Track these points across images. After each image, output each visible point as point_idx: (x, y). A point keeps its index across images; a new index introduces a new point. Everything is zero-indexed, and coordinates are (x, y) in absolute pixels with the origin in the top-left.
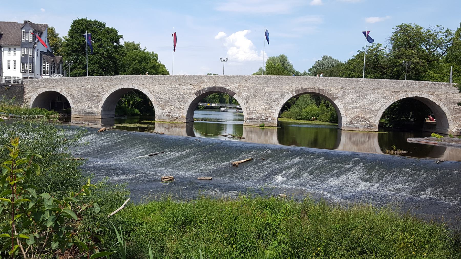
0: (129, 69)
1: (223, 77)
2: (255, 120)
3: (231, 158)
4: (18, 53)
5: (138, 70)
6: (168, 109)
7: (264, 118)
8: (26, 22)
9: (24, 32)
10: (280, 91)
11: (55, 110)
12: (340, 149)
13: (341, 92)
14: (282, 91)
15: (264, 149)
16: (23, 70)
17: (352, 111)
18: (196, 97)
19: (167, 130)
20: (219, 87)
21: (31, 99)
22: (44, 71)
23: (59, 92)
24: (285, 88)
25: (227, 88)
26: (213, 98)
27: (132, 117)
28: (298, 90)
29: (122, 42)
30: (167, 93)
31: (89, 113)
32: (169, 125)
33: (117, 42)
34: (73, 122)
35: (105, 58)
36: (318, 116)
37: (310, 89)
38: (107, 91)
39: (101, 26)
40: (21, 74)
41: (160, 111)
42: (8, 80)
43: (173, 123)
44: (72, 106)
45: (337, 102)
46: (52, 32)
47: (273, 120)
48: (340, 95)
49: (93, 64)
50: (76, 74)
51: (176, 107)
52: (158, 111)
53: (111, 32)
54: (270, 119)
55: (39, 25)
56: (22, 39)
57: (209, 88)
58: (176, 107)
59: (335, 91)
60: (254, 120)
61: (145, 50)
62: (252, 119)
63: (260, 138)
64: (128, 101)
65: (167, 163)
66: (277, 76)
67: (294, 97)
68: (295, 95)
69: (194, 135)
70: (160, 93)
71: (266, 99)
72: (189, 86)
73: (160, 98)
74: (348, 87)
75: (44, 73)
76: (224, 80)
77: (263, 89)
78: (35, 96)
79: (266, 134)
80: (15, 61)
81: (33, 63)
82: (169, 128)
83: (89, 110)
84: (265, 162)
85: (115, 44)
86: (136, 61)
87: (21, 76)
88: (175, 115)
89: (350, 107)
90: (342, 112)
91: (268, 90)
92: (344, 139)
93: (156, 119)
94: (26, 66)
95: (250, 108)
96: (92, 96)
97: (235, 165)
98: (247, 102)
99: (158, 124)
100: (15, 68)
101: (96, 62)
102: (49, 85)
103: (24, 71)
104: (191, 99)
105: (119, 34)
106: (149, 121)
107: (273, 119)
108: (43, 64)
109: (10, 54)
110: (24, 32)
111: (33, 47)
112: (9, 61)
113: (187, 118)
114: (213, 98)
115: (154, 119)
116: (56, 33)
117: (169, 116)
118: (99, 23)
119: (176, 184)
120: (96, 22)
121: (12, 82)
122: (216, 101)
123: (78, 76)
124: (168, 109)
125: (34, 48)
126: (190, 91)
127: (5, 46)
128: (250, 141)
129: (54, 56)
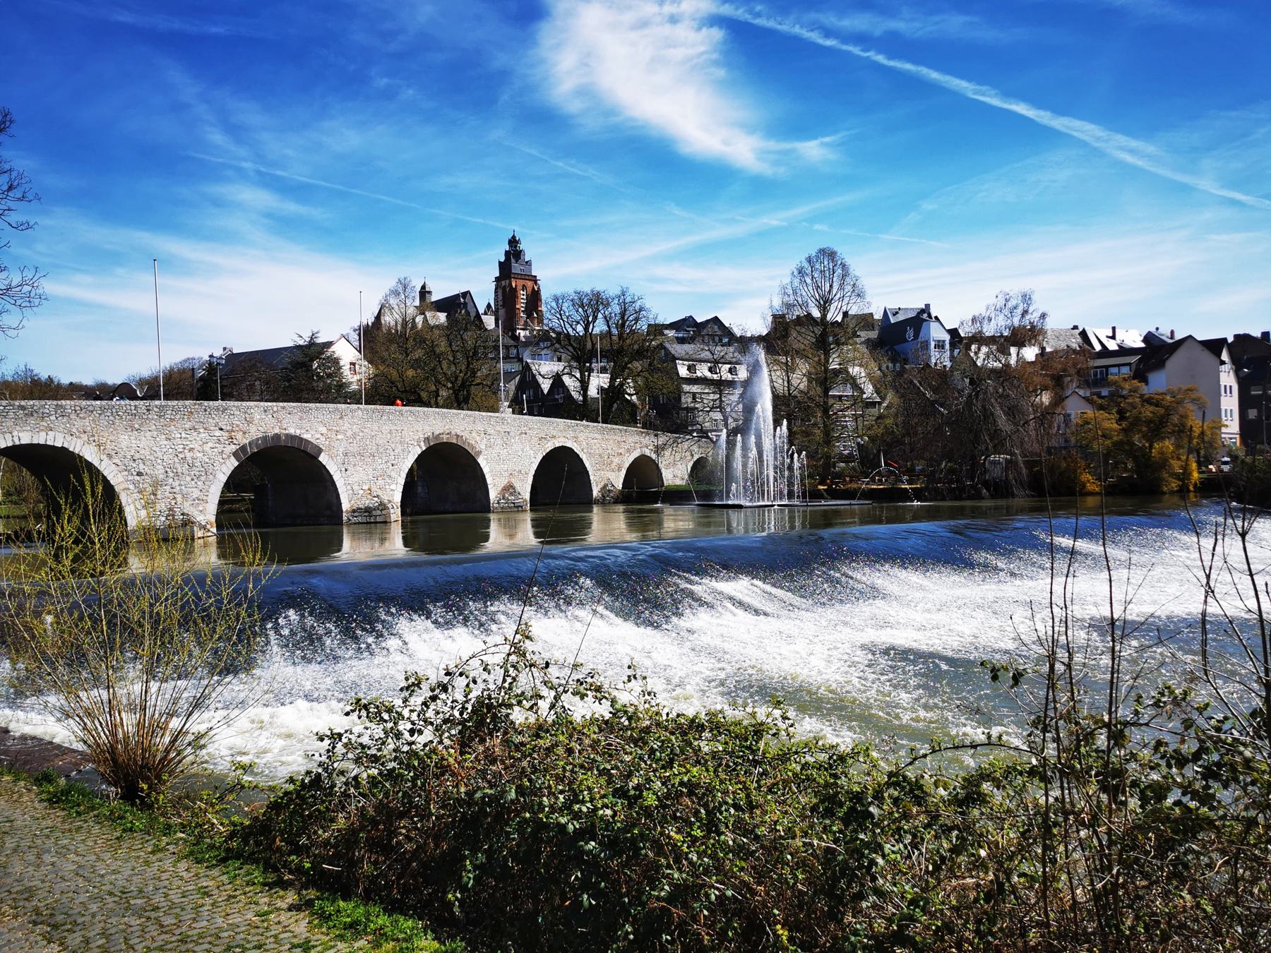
25: (305, 436)
30: (160, 454)
57: (265, 438)
70: (137, 456)
72: (218, 433)
73: (139, 474)
126: (220, 448)
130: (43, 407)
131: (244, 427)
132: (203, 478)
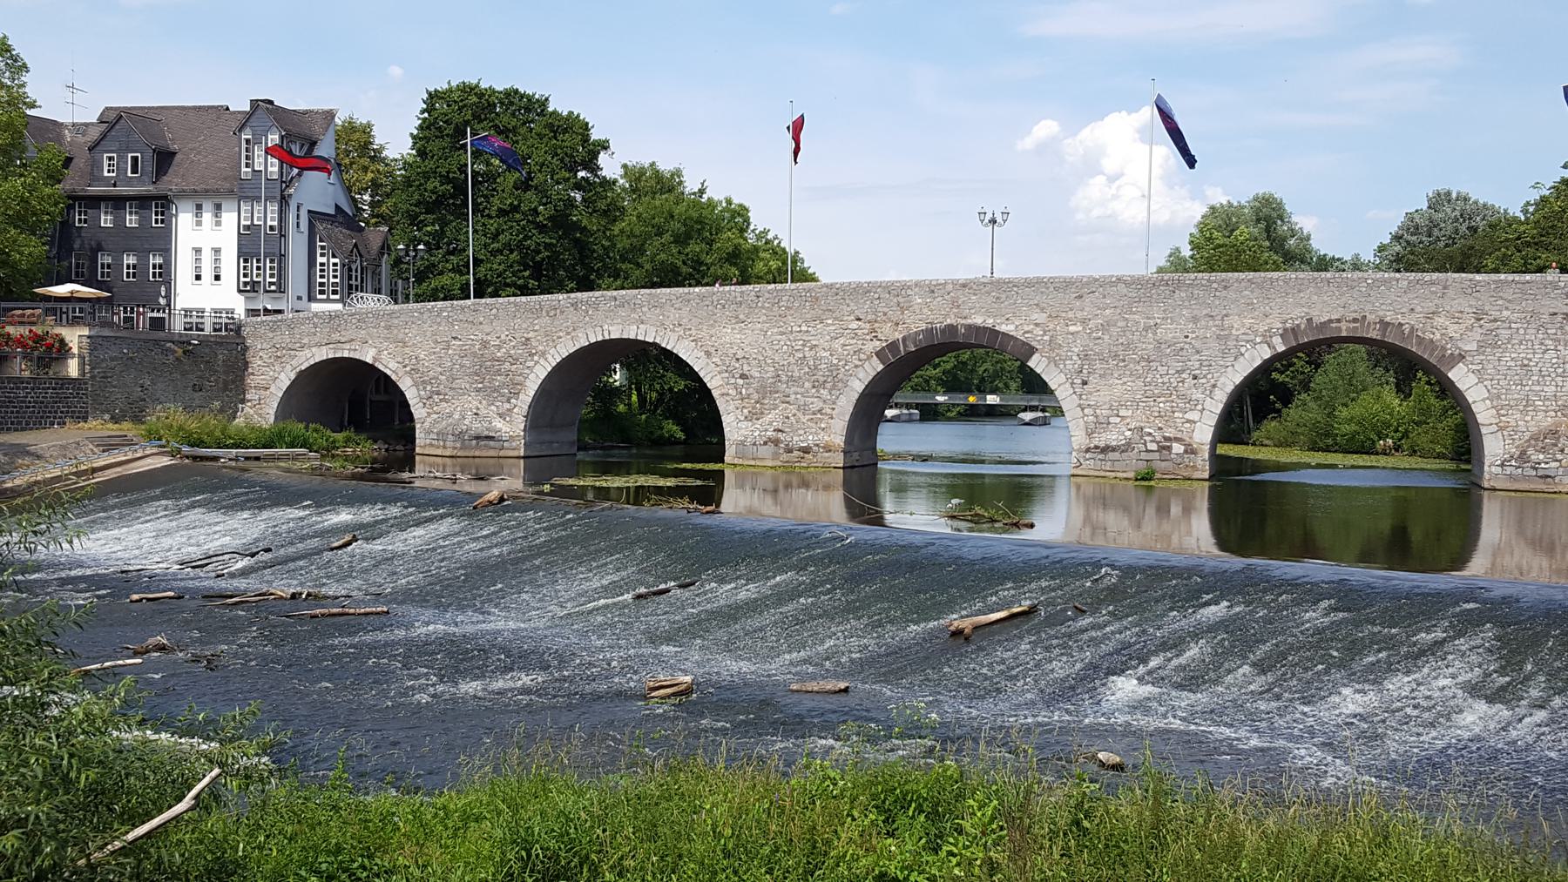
0: (639, 265)
1: (985, 285)
2: (1116, 455)
3: (950, 606)
4: (229, 218)
5: (675, 271)
6: (772, 418)
7: (1153, 447)
8: (255, 104)
9: (248, 141)
10: (1218, 337)
11: (358, 430)
12: (1478, 566)
13: (1477, 334)
14: (1227, 337)
15: (1097, 565)
16: (246, 284)
17: (1524, 412)
18: (881, 367)
19: (769, 500)
20: (969, 327)
21: (273, 389)
22: (322, 284)
23: (369, 360)
24: (1238, 324)
25: (1004, 328)
26: (997, 375)
27: (654, 451)
28: (1294, 331)
29: (609, 166)
31: (478, 438)
32: (775, 480)
33: (591, 164)
34: (424, 475)
35: (541, 228)
36: (1406, 435)
37: (1343, 326)
38: (543, 354)
39: (534, 106)
40: (241, 298)
41: (743, 425)
42: (194, 320)
43: (793, 472)
44: (418, 411)
45: (1460, 376)
46: (358, 140)
47: (1194, 452)
48: (1474, 346)
49: (494, 253)
50: (436, 290)
51: (803, 409)
52: (735, 427)
53: (565, 131)
54: (1178, 448)
55: (306, 112)
56: (244, 169)
58: (803, 409)
59: (1453, 330)
60: (1111, 455)
61: (702, 192)
62: (1106, 450)
63: (1139, 527)
64: (639, 390)
65: (696, 628)
66: (1206, 275)
67: (1277, 357)
68: (1281, 348)
69: (878, 521)
70: (740, 354)
71: (1163, 370)
72: (854, 325)
73: (743, 376)
74: (1505, 313)
75: (322, 292)
76: (990, 299)
77: (1146, 329)
78: (285, 379)
79: (1163, 510)
80: (217, 251)
81: (282, 257)
82: (776, 491)
83: (478, 427)
84: (1085, 621)
85: (581, 174)
86: (667, 237)
87: (239, 305)
88: (798, 441)
89: (1517, 393)
90: (1484, 414)
91: (1168, 332)
92: (1493, 527)
93: (727, 459)
94: (258, 268)
95: (1095, 407)
96: (489, 374)
97: (958, 633)
98: (1085, 383)
99: (738, 475)
100: (217, 278)
101: (507, 245)
102: (336, 336)
103: (249, 288)
104: (861, 375)
105: (595, 135)
106: (700, 466)
107: (1190, 451)
108: (320, 260)
109: (199, 223)
110: (248, 141)
111: (283, 197)
112: (198, 251)
113: (845, 452)
114: (958, 369)
115: (720, 458)
116: (378, 140)
117: (776, 442)
118: (522, 96)
119: (696, 711)
120: (511, 95)
121: (208, 330)
122: (1007, 386)
123: (445, 299)
124: (772, 418)
125: (284, 201)
127: (184, 195)
128: (1100, 541)
129: (361, 229)
130: (635, 297)
131: (895, 315)
132: (828, 386)
